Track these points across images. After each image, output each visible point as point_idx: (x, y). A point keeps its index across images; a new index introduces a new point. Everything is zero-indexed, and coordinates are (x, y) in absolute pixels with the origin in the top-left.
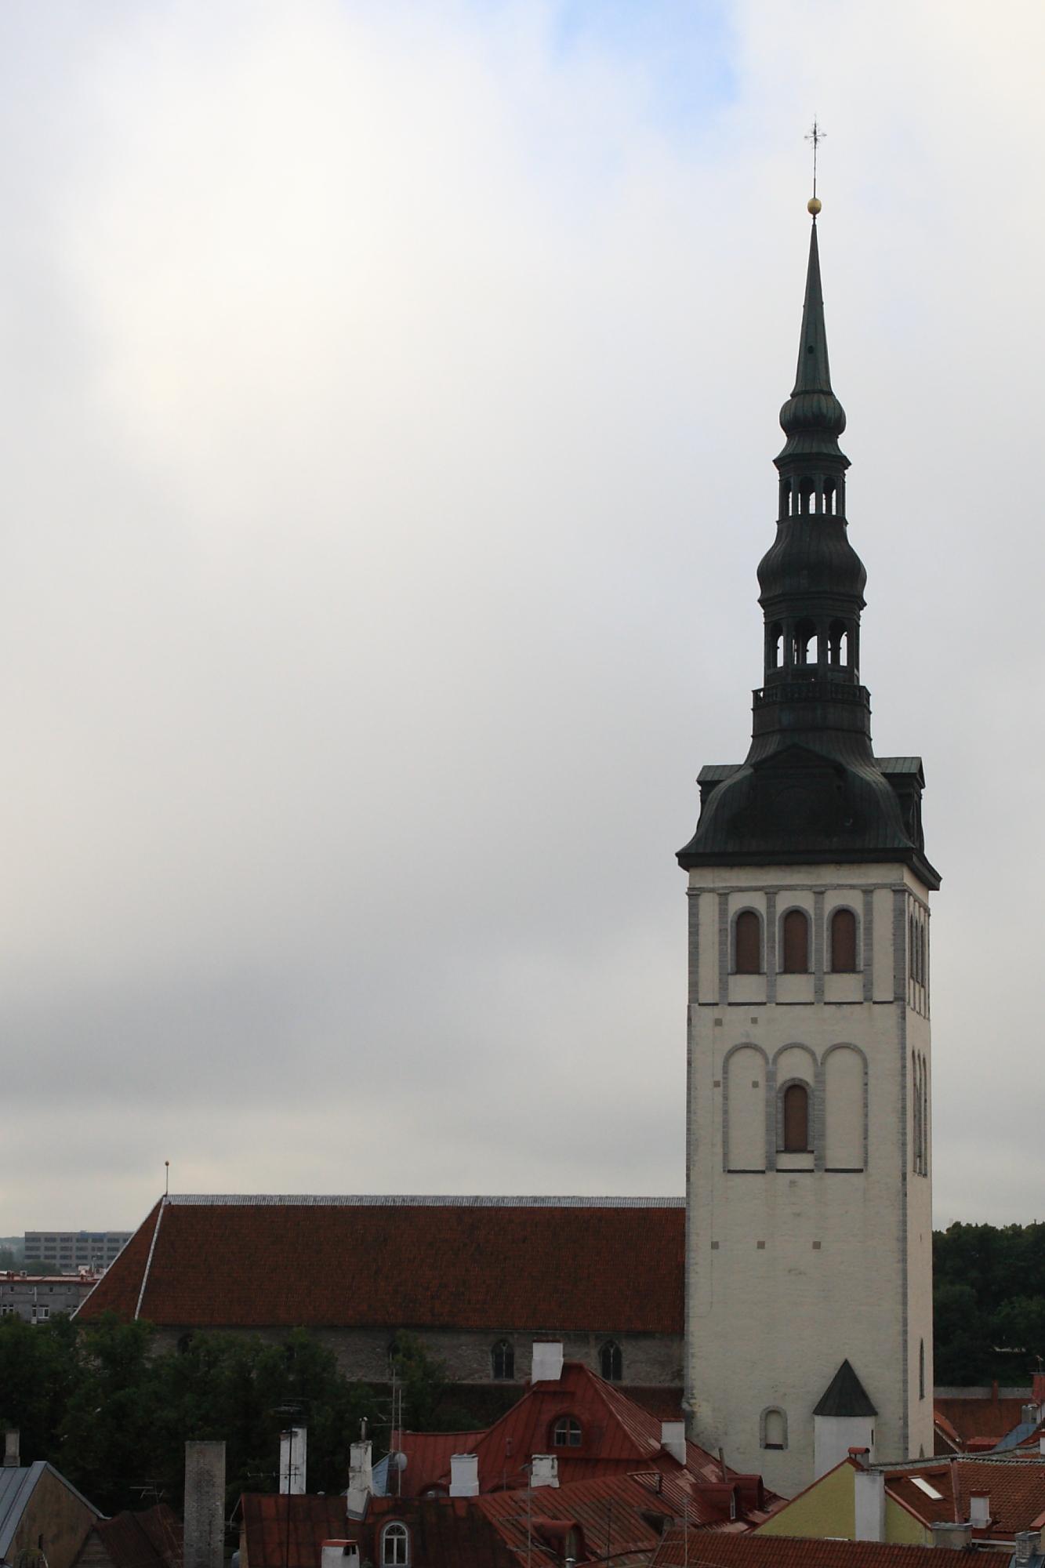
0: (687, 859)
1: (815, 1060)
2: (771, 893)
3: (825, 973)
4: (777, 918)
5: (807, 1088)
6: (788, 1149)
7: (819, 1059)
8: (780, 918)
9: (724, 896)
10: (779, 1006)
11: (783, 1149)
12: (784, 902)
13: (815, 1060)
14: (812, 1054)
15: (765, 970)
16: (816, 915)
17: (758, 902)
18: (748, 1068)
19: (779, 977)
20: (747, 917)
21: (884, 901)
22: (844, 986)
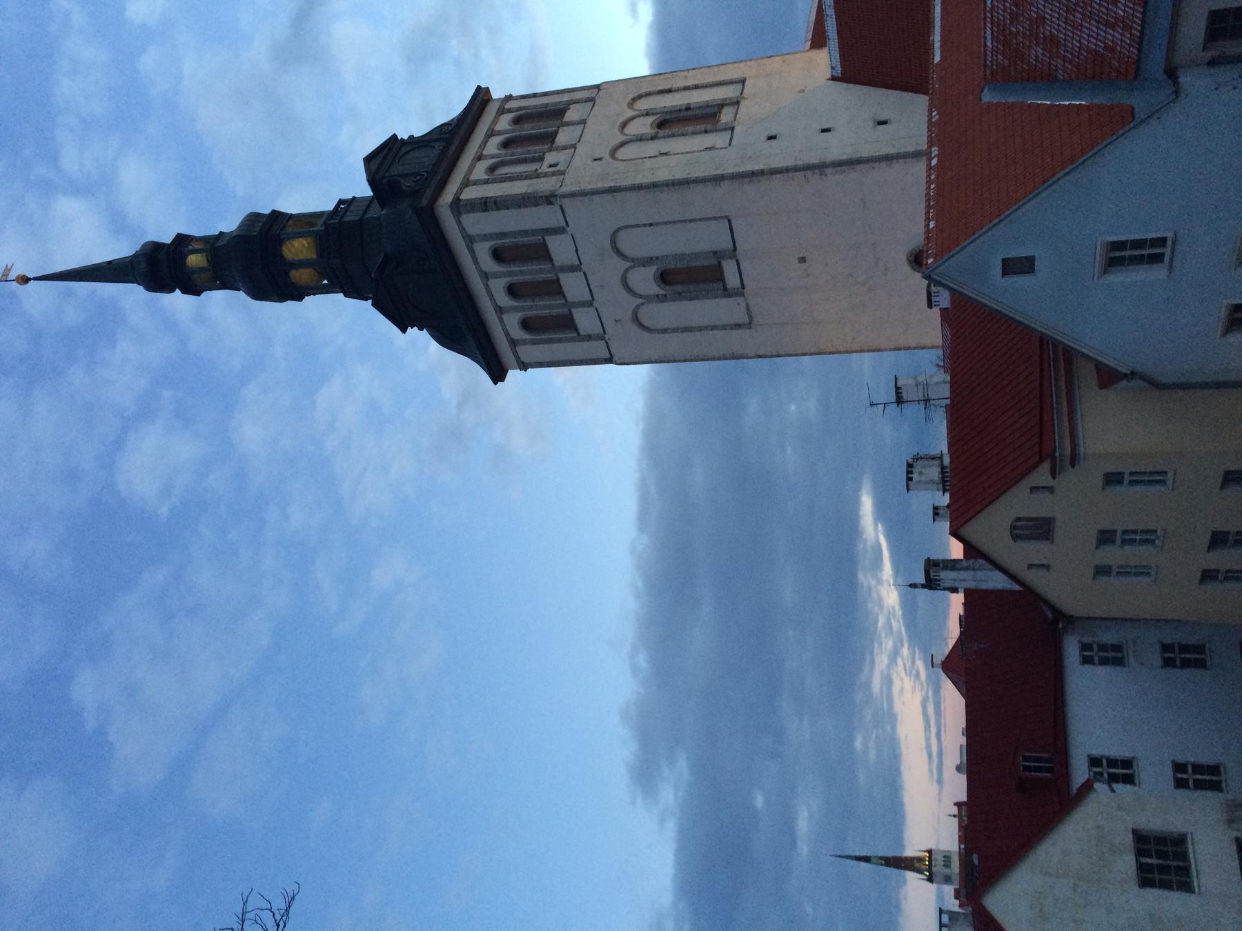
0: (498, 375)
1: (631, 268)
2: (500, 311)
3: (553, 265)
4: (517, 304)
5: (663, 269)
6: (721, 279)
7: (628, 264)
8: (517, 302)
9: (513, 343)
10: (595, 298)
11: (721, 284)
12: (504, 300)
13: (631, 268)
14: (627, 270)
15: (567, 310)
16: (505, 277)
17: (512, 322)
18: (652, 314)
19: (568, 299)
20: (526, 325)
21: (476, 223)
22: (560, 249)
